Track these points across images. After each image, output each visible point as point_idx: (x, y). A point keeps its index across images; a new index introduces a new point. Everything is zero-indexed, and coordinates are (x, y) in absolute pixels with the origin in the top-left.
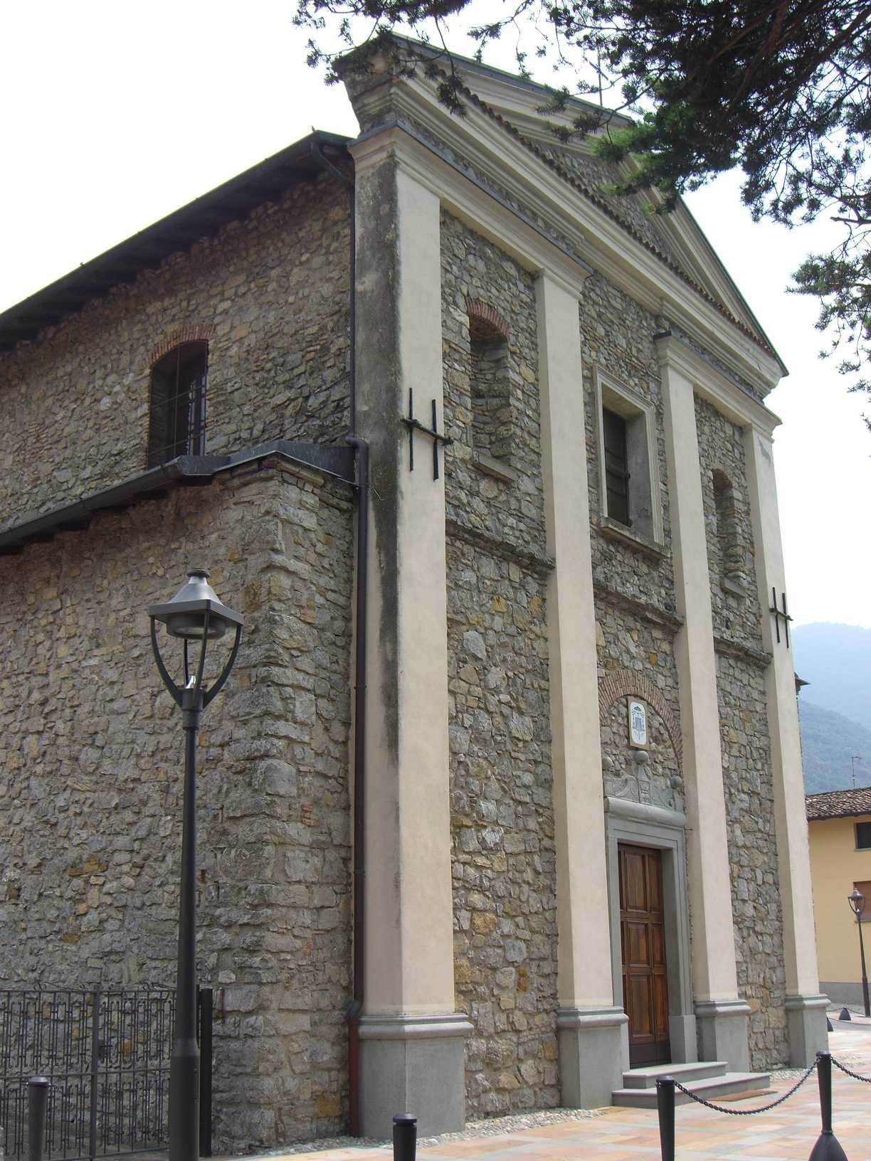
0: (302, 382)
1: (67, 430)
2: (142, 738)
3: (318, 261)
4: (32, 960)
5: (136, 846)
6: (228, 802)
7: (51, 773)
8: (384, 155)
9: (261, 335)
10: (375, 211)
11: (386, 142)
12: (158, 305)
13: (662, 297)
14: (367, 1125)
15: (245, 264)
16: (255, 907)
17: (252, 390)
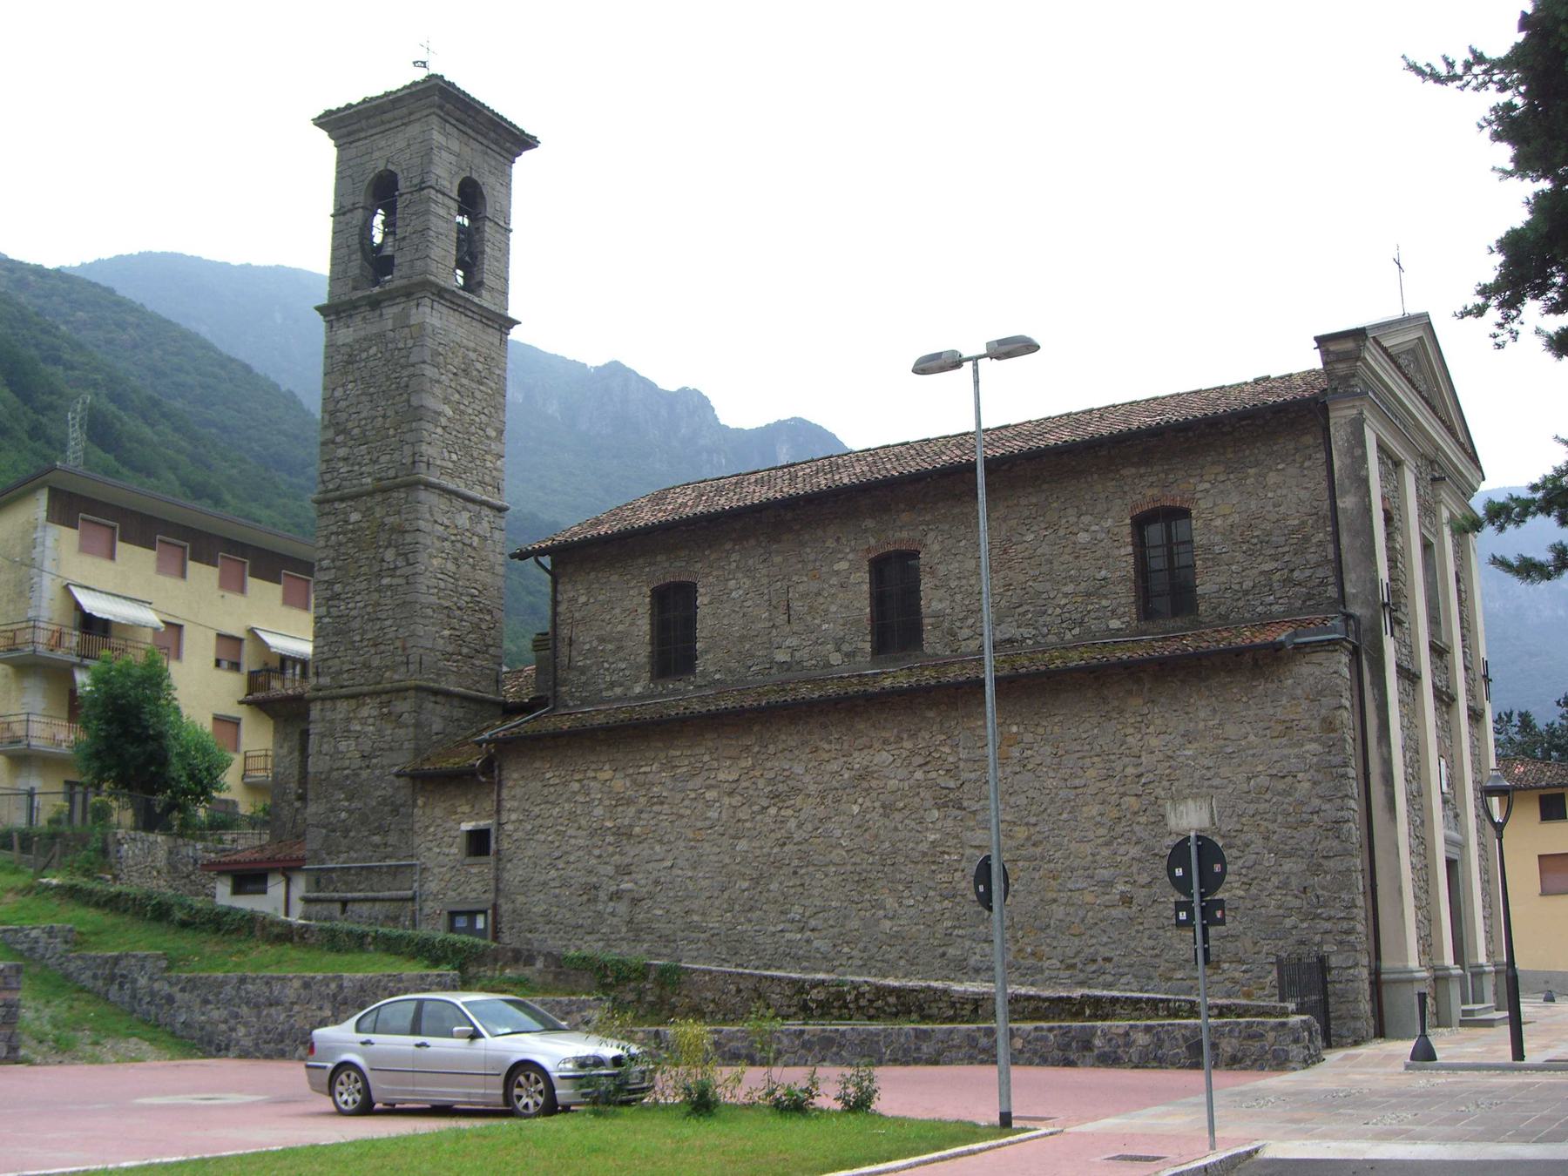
0: (1286, 558)
1: (1039, 551)
2: (1242, 805)
3: (1292, 470)
4: (1151, 943)
5: (1244, 871)
6: (1320, 847)
7: (1153, 823)
8: (1355, 411)
9: (1245, 516)
10: (1350, 451)
11: (1357, 403)
12: (1133, 470)
13: (1438, 448)
14: (1387, 1031)
15: (1222, 458)
16: (1346, 908)
17: (1239, 556)
